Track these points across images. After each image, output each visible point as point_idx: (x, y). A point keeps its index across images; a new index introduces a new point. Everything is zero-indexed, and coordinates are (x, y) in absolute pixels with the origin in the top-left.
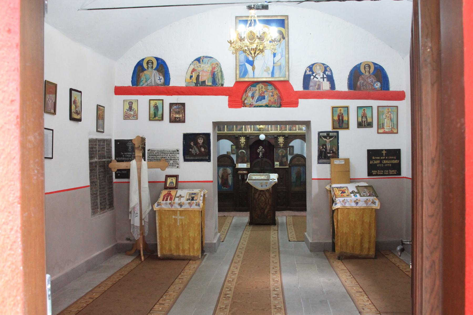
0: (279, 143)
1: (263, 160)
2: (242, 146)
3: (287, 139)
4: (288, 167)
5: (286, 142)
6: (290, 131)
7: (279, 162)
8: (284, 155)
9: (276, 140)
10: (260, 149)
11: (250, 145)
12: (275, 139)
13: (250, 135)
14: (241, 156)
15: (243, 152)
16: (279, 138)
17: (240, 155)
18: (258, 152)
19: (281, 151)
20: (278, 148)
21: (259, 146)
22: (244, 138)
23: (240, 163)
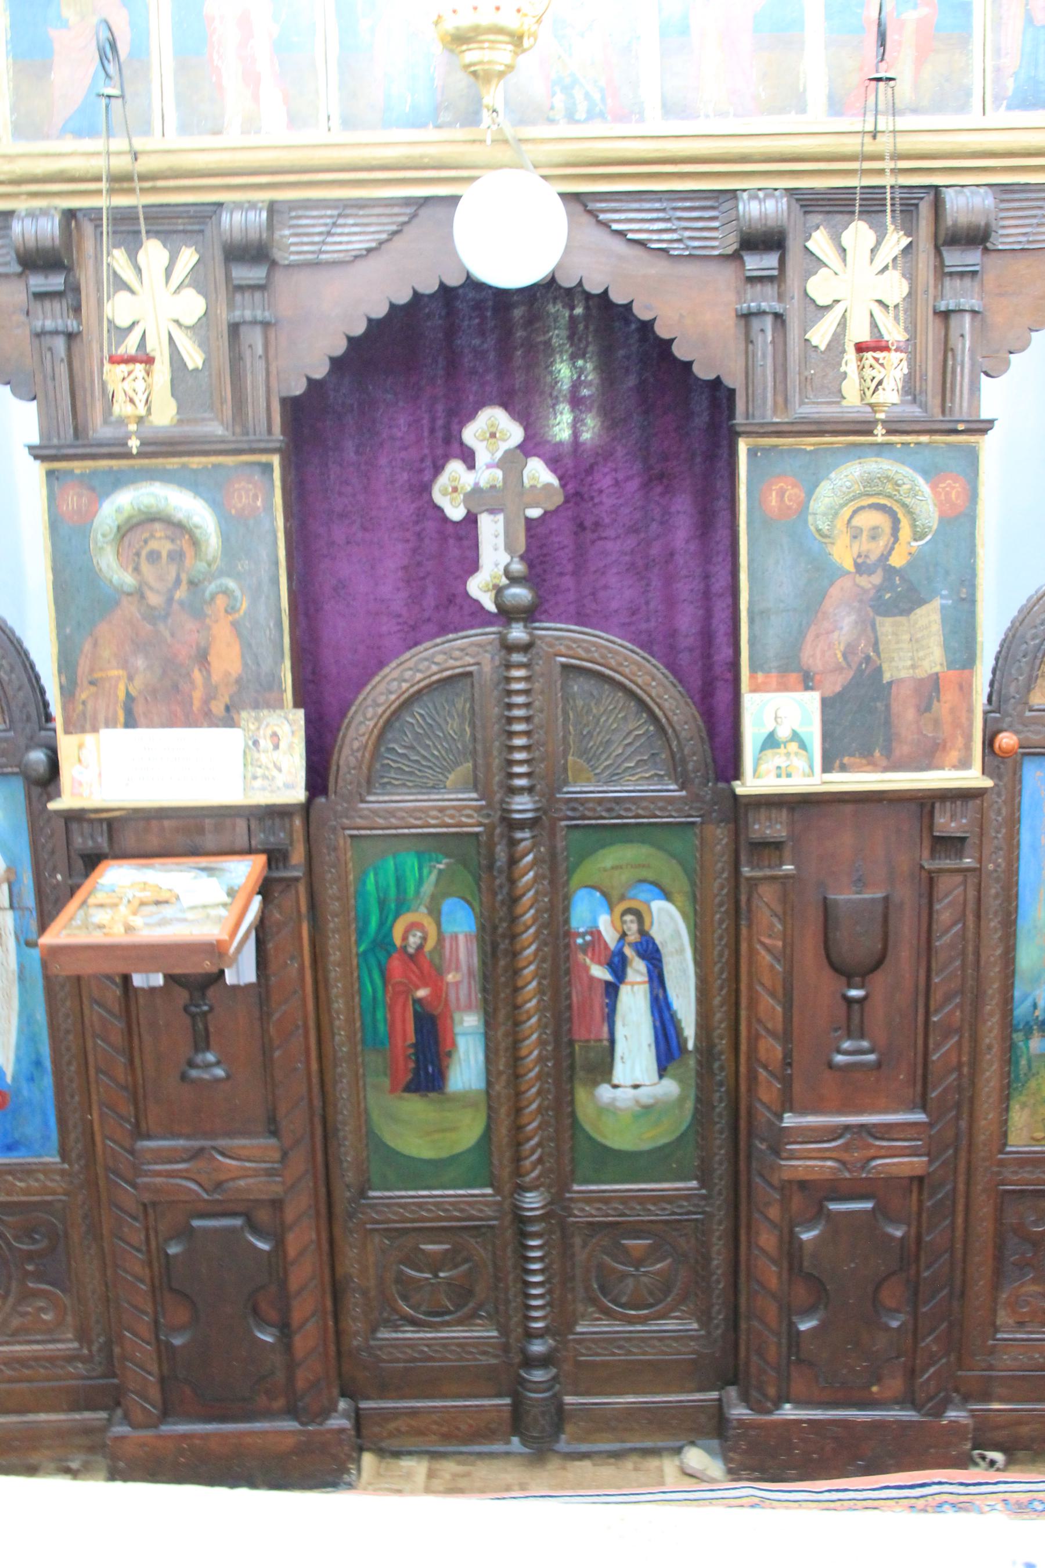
0: (820, 335)
1: (526, 648)
2: (121, 408)
3: (972, 258)
4: (973, 777)
5: (945, 315)
6: (1009, 108)
7: (812, 700)
8: (915, 560)
9: (777, 279)
10: (482, 457)
11: (299, 388)
12: (757, 263)
13: (272, 208)
14: (139, 594)
15: (179, 528)
16: (820, 242)
17: (126, 579)
18: (456, 513)
19: (871, 485)
20: (809, 442)
21: (472, 416)
22: (188, 257)
23: (130, 722)
